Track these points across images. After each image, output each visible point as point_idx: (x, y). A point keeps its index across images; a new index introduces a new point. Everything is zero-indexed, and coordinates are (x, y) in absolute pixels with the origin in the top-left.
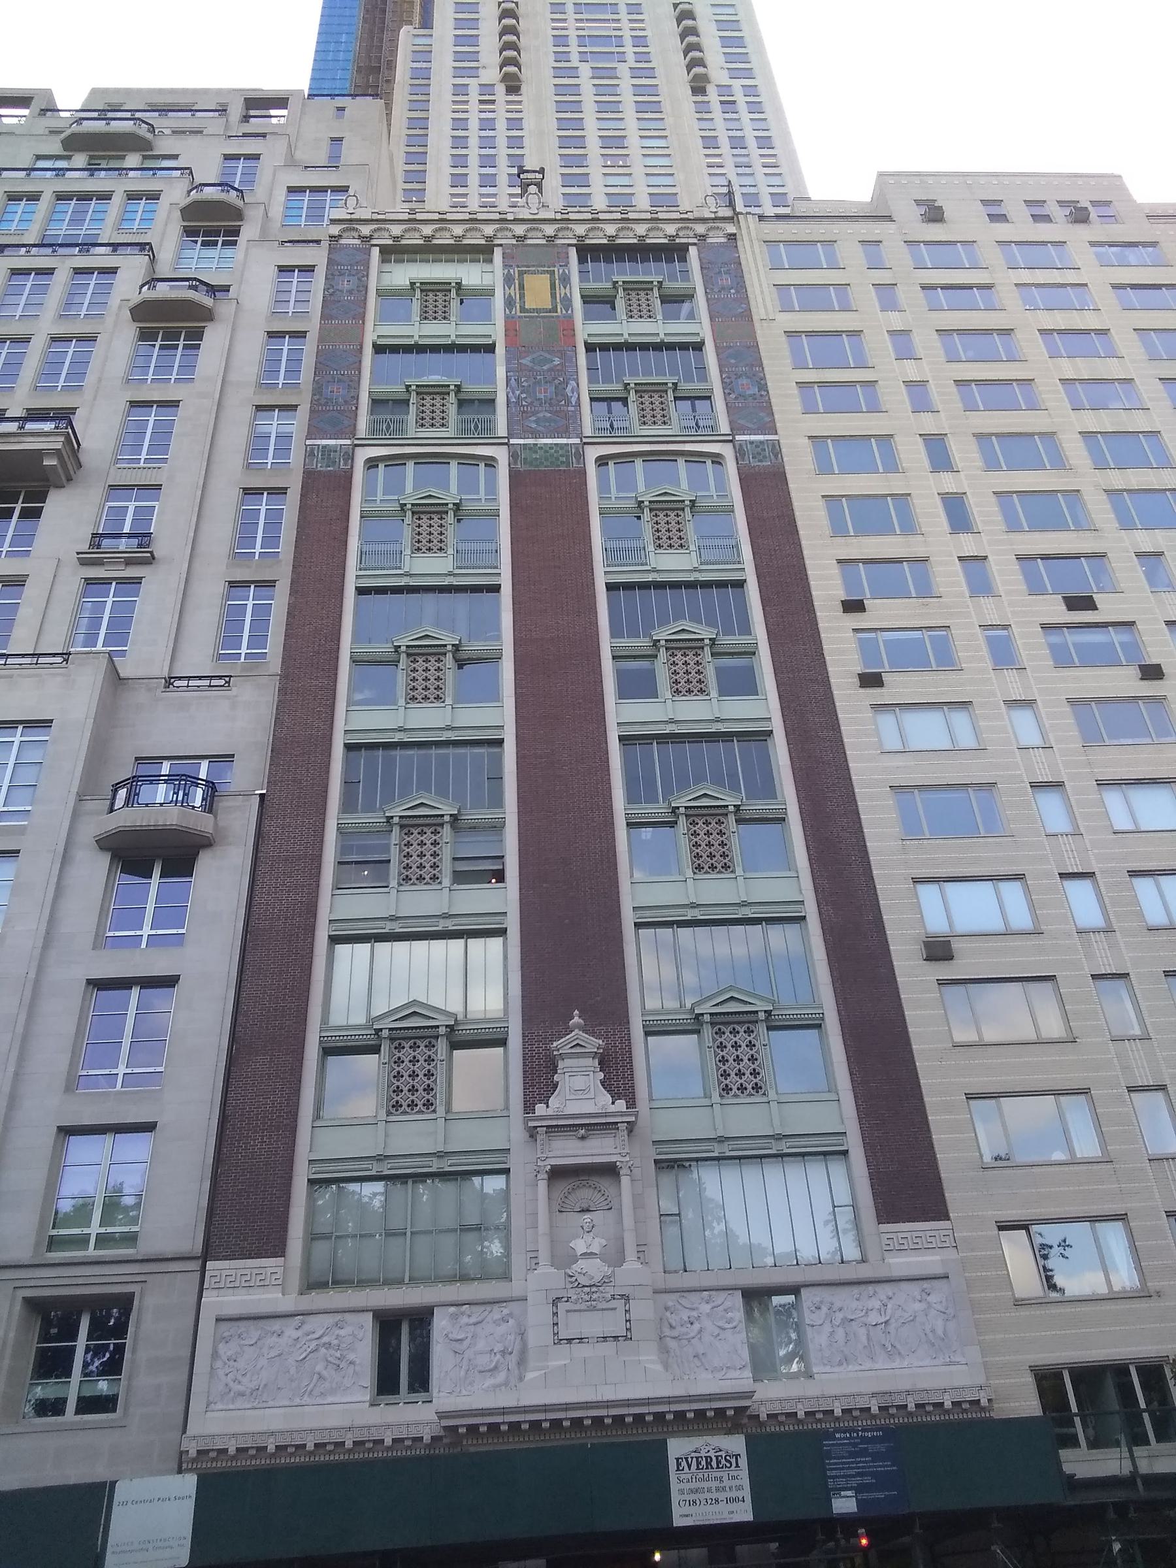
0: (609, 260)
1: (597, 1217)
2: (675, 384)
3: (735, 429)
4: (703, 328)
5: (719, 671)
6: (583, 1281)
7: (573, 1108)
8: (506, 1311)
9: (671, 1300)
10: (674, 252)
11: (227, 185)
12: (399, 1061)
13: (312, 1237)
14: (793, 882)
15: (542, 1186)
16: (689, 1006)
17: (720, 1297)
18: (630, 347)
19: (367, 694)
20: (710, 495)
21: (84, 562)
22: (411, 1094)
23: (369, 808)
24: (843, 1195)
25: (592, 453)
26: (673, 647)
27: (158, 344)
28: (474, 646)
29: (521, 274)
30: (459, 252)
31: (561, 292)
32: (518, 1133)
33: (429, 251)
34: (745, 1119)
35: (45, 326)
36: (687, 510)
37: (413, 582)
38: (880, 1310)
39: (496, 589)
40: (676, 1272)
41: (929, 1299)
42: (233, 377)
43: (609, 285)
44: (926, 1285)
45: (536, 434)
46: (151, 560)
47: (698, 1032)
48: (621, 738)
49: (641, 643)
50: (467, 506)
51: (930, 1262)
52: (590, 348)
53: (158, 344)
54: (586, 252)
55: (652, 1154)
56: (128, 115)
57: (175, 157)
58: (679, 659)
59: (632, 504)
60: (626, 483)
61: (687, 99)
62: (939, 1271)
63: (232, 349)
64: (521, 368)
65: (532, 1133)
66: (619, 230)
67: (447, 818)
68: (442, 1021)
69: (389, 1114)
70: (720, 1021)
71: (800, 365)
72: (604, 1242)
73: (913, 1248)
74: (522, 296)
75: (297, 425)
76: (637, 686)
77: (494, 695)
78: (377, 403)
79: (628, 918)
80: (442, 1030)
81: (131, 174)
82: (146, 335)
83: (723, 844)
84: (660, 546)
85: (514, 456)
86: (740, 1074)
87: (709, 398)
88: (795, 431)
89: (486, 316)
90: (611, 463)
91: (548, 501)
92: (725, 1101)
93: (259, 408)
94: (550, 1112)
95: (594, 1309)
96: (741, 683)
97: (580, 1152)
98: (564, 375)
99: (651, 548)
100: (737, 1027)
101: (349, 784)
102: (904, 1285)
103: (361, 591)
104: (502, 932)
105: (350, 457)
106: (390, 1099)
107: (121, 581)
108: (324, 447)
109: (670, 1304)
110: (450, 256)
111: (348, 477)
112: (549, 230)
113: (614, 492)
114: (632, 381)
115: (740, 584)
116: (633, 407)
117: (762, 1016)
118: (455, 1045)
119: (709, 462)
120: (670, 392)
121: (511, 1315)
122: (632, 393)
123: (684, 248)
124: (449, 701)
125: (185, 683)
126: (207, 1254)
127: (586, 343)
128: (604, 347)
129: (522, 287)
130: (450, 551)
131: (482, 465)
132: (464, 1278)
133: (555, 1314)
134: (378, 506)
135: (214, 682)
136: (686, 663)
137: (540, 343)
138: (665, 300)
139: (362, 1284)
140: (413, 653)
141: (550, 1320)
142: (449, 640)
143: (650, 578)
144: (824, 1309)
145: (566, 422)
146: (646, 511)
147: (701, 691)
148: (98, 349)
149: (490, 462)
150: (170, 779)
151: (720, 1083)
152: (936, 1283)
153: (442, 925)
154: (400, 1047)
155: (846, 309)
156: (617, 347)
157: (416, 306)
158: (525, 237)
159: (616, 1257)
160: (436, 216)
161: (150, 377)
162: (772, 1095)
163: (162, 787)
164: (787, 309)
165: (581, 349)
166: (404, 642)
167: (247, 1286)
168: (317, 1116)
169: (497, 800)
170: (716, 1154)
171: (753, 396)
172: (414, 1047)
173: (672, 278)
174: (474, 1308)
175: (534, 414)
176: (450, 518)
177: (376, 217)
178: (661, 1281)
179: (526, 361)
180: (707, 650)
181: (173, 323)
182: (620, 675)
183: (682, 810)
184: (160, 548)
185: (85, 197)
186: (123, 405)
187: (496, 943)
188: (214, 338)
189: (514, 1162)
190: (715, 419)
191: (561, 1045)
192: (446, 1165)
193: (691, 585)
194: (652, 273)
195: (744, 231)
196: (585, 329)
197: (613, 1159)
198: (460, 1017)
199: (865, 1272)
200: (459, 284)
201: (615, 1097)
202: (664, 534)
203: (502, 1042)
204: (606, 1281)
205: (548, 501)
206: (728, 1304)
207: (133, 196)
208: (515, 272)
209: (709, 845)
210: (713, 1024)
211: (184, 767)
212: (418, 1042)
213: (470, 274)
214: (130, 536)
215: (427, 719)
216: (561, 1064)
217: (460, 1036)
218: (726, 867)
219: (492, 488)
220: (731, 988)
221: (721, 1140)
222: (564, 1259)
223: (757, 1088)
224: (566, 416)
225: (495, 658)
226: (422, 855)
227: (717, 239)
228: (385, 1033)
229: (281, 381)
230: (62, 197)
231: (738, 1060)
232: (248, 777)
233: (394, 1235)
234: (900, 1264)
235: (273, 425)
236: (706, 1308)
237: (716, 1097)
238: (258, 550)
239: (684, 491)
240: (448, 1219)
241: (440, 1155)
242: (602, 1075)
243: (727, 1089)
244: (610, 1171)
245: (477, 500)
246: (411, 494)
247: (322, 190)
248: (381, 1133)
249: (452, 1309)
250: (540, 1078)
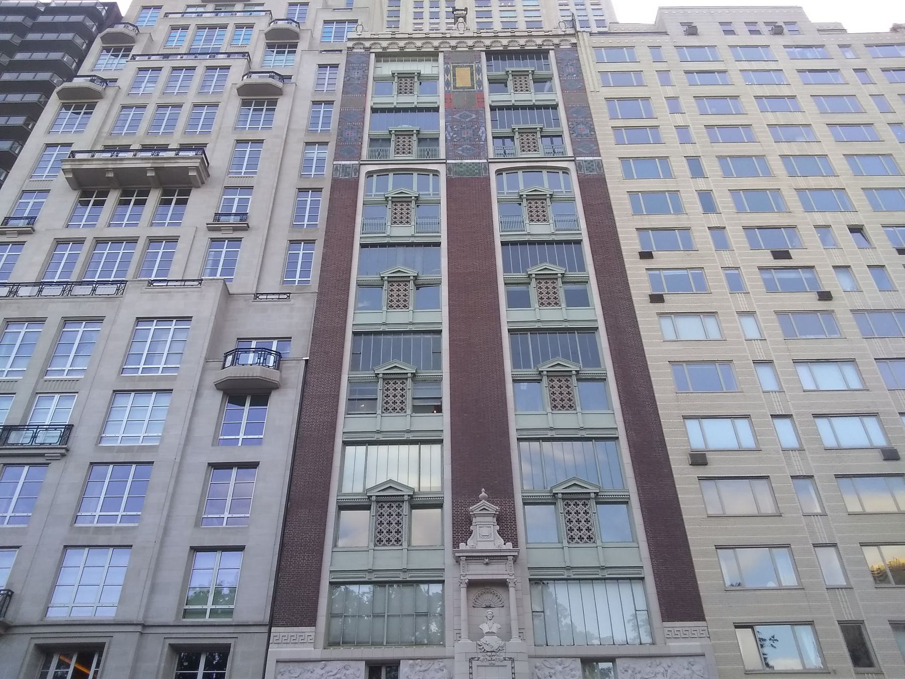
0: (503, 59)
1: (495, 611)
2: (541, 129)
3: (576, 153)
4: (557, 97)
5: (566, 292)
6: (487, 648)
7: (481, 546)
8: (442, 664)
9: (538, 662)
10: (541, 54)
12: (381, 515)
13: (331, 615)
14: (610, 416)
15: (464, 591)
16: (549, 489)
17: (568, 662)
18: (516, 108)
19: (366, 304)
20: (561, 192)
21: (211, 229)
22: (388, 534)
23: (366, 368)
24: (641, 604)
25: (493, 168)
26: (540, 278)
27: (252, 108)
28: (424, 277)
29: (454, 67)
30: (419, 55)
31: (476, 77)
32: (449, 560)
33: (402, 55)
34: (583, 556)
35: (191, 98)
36: (548, 200)
37: (392, 241)
38: (663, 674)
39: (438, 244)
40: (542, 646)
41: (693, 668)
42: (293, 126)
43: (504, 73)
44: (691, 659)
45: (462, 158)
46: (247, 228)
47: (554, 504)
48: (509, 330)
49: (521, 276)
50: (422, 198)
51: (693, 646)
52: (493, 109)
53: (252, 108)
54: (491, 55)
55: (528, 575)
57: (262, 4)
58: (543, 285)
59: (516, 196)
60: (513, 185)
62: (699, 651)
63: (293, 111)
64: (454, 120)
65: (458, 560)
66: (509, 42)
67: (409, 375)
68: (406, 492)
69: (375, 545)
70: (568, 498)
71: (613, 117)
72: (499, 626)
73: (683, 637)
74: (455, 80)
75: (328, 153)
76: (519, 300)
77: (437, 305)
78: (373, 140)
79: (513, 435)
80: (406, 498)
81: (238, 14)
82: (245, 103)
83: (569, 393)
84: (532, 220)
85: (449, 170)
86: (580, 530)
87: (561, 136)
88: (611, 155)
89: (434, 92)
90: (504, 174)
91: (468, 193)
92: (571, 545)
93: (307, 144)
94: (468, 548)
95: (493, 665)
96: (579, 299)
97: (485, 572)
98: (479, 123)
99: (527, 221)
100: (578, 502)
101: (355, 354)
102: (679, 659)
103: (363, 246)
104: (440, 442)
105: (358, 171)
106: (376, 537)
107: (231, 240)
109: (538, 664)
110: (414, 58)
111: (357, 181)
112: (470, 42)
113: (506, 191)
114: (516, 127)
115: (579, 242)
116: (517, 142)
117: (593, 495)
118: (414, 507)
119: (561, 172)
120: (538, 133)
121: (444, 666)
122: (517, 133)
123: (547, 52)
124: (411, 308)
125: (265, 297)
126: (271, 624)
127: (490, 106)
128: (501, 108)
129: (454, 75)
130: (413, 223)
131: (431, 175)
132: (418, 644)
133: (471, 667)
134: (373, 198)
135: (281, 297)
136: (547, 288)
137: (465, 106)
138: (536, 81)
139: (360, 644)
140: (392, 281)
141: (467, 670)
142: (411, 273)
143: (526, 238)
144: (630, 672)
145: (478, 149)
146: (524, 200)
147: (556, 304)
148: (219, 111)
149: (436, 173)
150: (256, 350)
151: (568, 535)
152: (697, 659)
153: (406, 437)
154: (382, 507)
155: (640, 84)
156: (508, 108)
157: (395, 86)
158: (456, 47)
159: (507, 635)
160: (407, 36)
161: (248, 126)
162: (599, 543)
163: (252, 355)
164: (606, 85)
165: (488, 109)
166: (386, 275)
168: (335, 545)
169: (438, 366)
170: (565, 577)
171: (587, 135)
172: (390, 507)
173: (540, 69)
174: (424, 662)
175: (460, 146)
176: (413, 204)
177: (373, 36)
178: (533, 651)
179: (456, 116)
180: (560, 280)
181: (260, 96)
182: (509, 294)
183: (545, 373)
184: (252, 222)
185: (213, 27)
186: (232, 142)
187: (436, 448)
188: (283, 104)
189: (447, 577)
190: (565, 148)
191: (474, 509)
192: (407, 577)
193: (550, 243)
194: (528, 66)
195: (581, 42)
196: (490, 98)
198: (416, 490)
199: (653, 650)
200: (419, 74)
201: (506, 540)
202: (534, 214)
203: (440, 506)
204: (500, 649)
205: (468, 193)
206: (572, 666)
207: (239, 26)
208: (451, 66)
209: (561, 393)
210: (563, 499)
211: (264, 344)
212: (393, 504)
213: (425, 68)
214: (236, 215)
215: (399, 318)
216: (474, 520)
217: (417, 501)
218: (571, 407)
219: (437, 188)
220: (574, 479)
221: (568, 568)
222: (476, 635)
223: (590, 538)
224: (479, 147)
225: (438, 284)
226: (395, 396)
227: (566, 46)
228: (374, 498)
229: (319, 129)
230: (200, 27)
231: (578, 521)
232: (299, 349)
233: (378, 616)
234: (675, 646)
235: (315, 153)
236: (559, 668)
237: (565, 543)
238: (306, 223)
239: (546, 189)
240: (409, 609)
241: (405, 571)
242: (498, 528)
243: (572, 538)
244: (503, 584)
245: (428, 195)
246: (391, 192)
247: (343, 22)
248: (371, 557)
249: (411, 661)
250: (462, 528)
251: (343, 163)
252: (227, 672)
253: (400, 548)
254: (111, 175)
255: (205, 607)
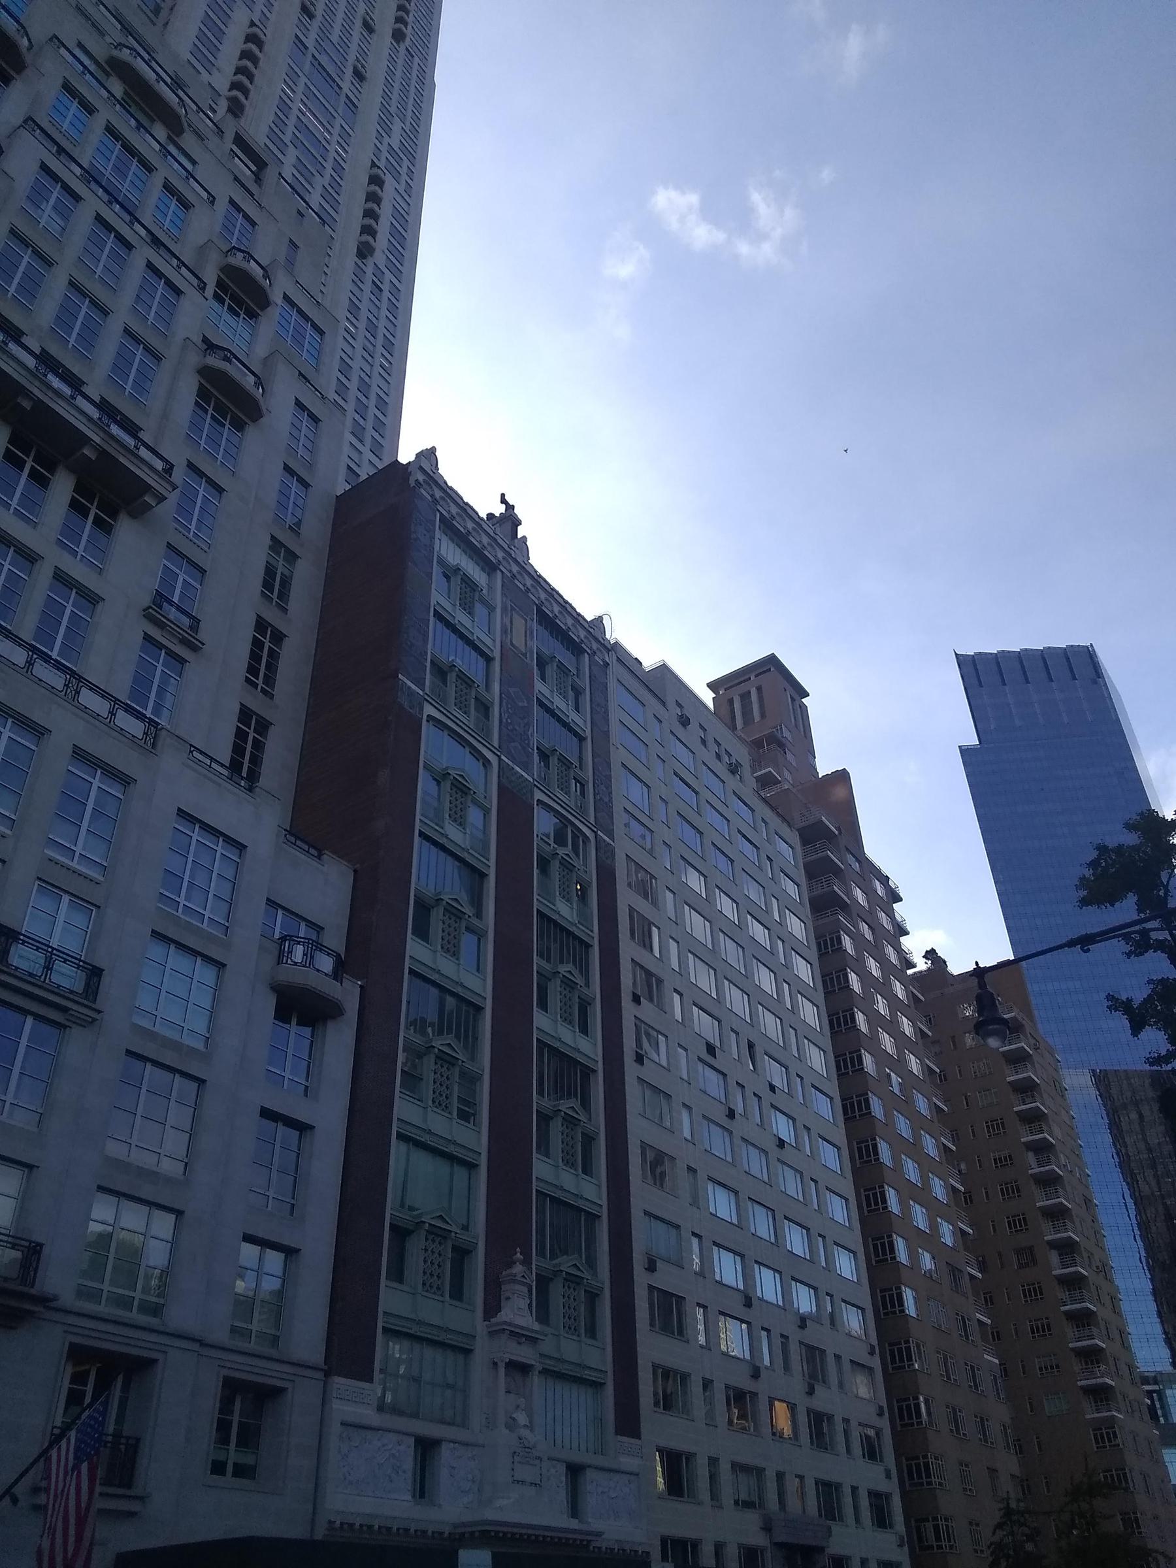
11: (24, 28)
56: (153, 64)
57: (194, 162)
61: (351, 258)
108: (409, 688)
167: (352, 1401)
179: (511, 690)
197: (533, 1363)
234: (628, 1463)
251: (409, 683)
252: (217, 1415)
253: (441, 1298)
254: (27, 404)
255: (132, 1294)
